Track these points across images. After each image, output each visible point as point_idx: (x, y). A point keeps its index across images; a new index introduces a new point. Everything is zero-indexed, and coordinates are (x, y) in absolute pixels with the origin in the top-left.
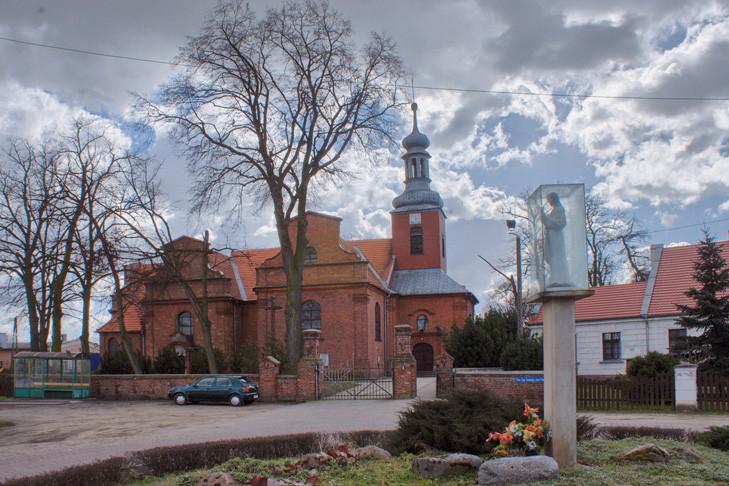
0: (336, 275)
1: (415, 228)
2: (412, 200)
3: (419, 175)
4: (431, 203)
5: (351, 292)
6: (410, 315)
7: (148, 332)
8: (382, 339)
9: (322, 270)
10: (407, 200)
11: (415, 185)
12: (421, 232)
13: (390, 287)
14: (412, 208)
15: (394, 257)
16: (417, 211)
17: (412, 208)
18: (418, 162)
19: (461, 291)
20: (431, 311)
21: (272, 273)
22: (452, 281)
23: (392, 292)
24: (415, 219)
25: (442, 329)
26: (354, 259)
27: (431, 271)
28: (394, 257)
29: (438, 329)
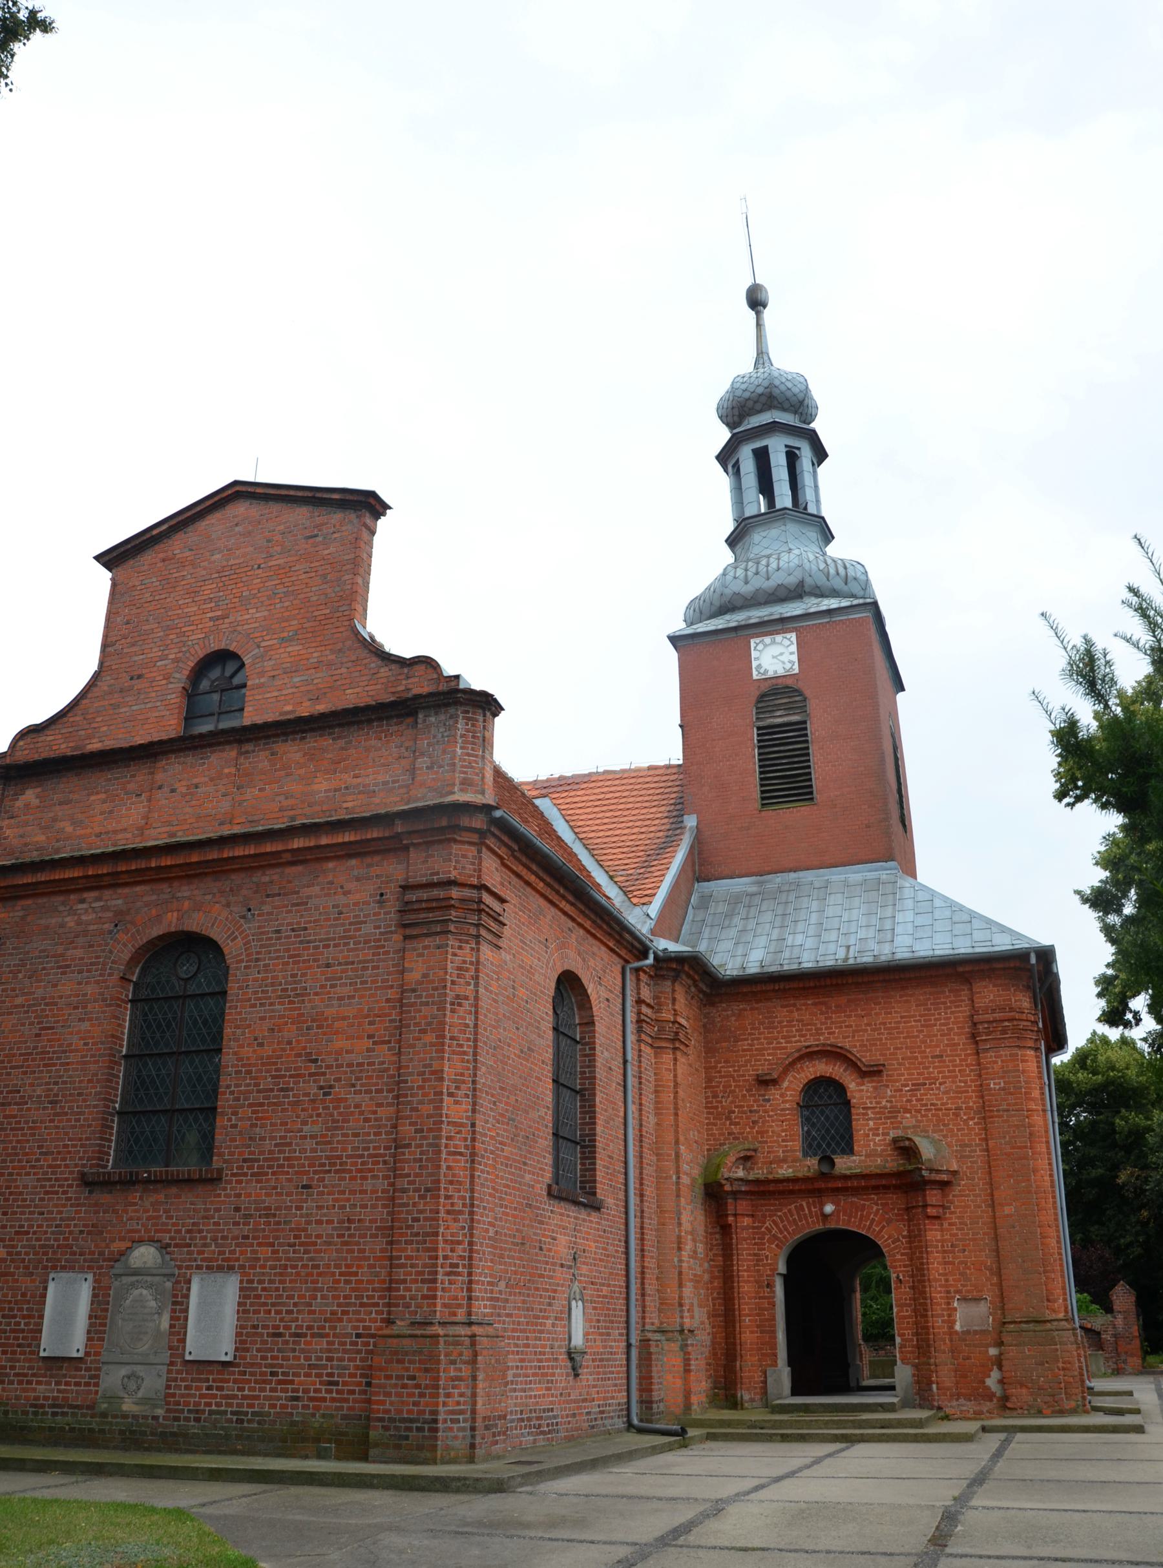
0: (322, 786)
2: (757, 583)
3: (784, 498)
4: (835, 593)
5: (393, 870)
6: (765, 1082)
8: (606, 1191)
9: (259, 759)
10: (739, 587)
11: (762, 541)
12: (803, 709)
13: (669, 922)
14: (756, 615)
15: (691, 821)
16: (780, 625)
17: (756, 615)
18: (778, 461)
19: (1002, 944)
20: (867, 1058)
21: (30, 796)
22: (954, 907)
23: (663, 944)
25: (927, 1150)
26: (420, 685)
27: (856, 874)
28: (691, 821)
29: (906, 1150)
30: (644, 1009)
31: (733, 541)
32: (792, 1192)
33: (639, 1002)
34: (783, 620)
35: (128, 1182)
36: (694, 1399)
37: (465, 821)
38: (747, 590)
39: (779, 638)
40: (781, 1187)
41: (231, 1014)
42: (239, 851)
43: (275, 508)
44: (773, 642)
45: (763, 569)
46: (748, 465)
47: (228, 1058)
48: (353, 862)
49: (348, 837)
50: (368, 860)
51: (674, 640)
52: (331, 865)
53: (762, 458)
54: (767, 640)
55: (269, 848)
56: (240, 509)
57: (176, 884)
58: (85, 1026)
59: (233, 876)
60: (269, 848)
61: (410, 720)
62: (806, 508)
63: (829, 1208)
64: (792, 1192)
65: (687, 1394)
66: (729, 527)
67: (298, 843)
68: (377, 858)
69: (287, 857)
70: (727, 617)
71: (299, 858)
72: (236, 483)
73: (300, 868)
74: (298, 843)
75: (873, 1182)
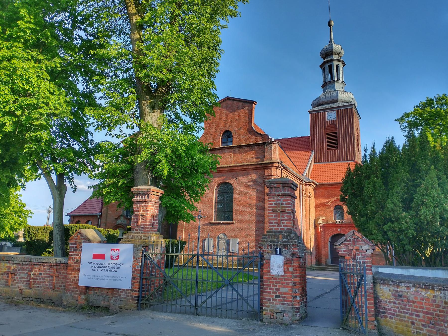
1: (332, 124)
7: (103, 215)
24: (331, 116)
30: (303, 192)
31: (323, 87)
32: (332, 226)
33: (302, 191)
34: (333, 108)
35: (219, 224)
36: (313, 263)
37: (274, 165)
38: (326, 101)
39: (332, 112)
40: (330, 225)
41: (234, 196)
42: (234, 168)
43: (235, 102)
44: (331, 113)
45: (329, 96)
46: (327, 69)
47: (234, 204)
48: (255, 171)
49: (254, 167)
50: (257, 171)
51: (309, 112)
52: (251, 171)
53: (330, 67)
54: (330, 112)
55: (240, 168)
56: (229, 102)
57: (223, 173)
58: (208, 197)
59: (233, 172)
60: (240, 168)
61: (264, 146)
62: (340, 80)
63: (339, 230)
64: (332, 226)
65: (311, 262)
66: (322, 84)
67: (245, 167)
68: (259, 170)
69: (243, 170)
70: (321, 107)
71: (245, 170)
72: (227, 97)
73: (245, 171)
74: (245, 167)
75: (348, 225)
